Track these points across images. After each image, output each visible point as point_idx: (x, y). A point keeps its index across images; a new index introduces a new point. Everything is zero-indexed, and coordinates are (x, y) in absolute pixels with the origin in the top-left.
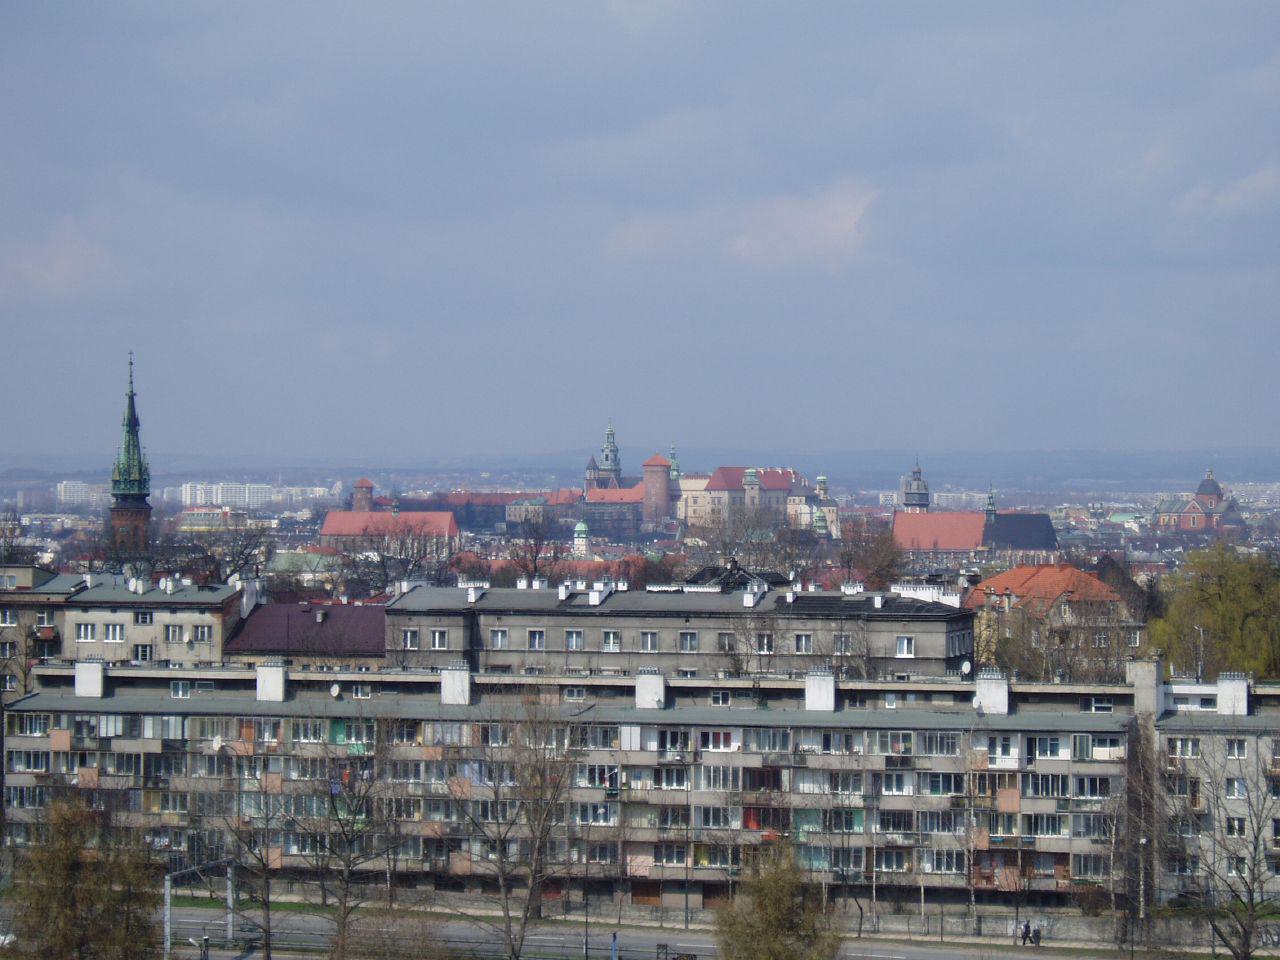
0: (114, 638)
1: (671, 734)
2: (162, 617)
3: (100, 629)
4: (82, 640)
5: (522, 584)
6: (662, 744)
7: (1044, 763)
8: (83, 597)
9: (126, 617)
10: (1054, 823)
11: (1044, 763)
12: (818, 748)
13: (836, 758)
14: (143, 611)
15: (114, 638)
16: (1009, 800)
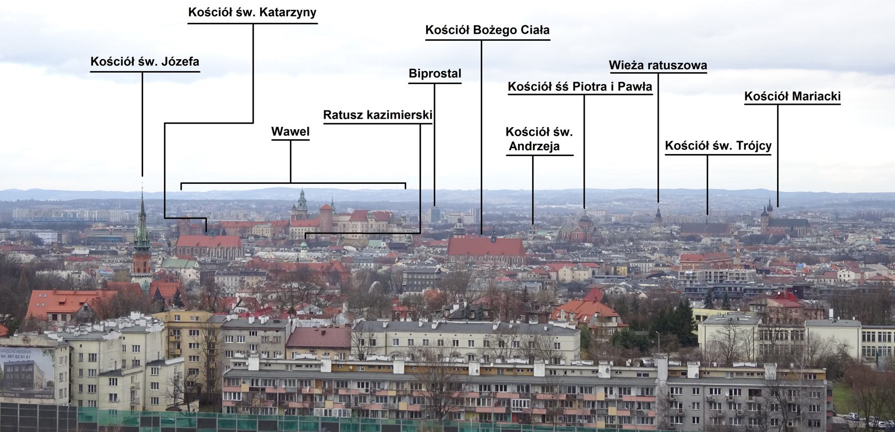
0: (241, 341)
1: (484, 387)
2: (261, 333)
3: (235, 338)
4: (228, 342)
5: (402, 320)
6: (481, 389)
7: (626, 398)
8: (227, 325)
9: (246, 333)
10: (629, 419)
11: (626, 398)
12: (540, 391)
13: (548, 396)
14: (253, 331)
15: (241, 341)
16: (612, 411)
